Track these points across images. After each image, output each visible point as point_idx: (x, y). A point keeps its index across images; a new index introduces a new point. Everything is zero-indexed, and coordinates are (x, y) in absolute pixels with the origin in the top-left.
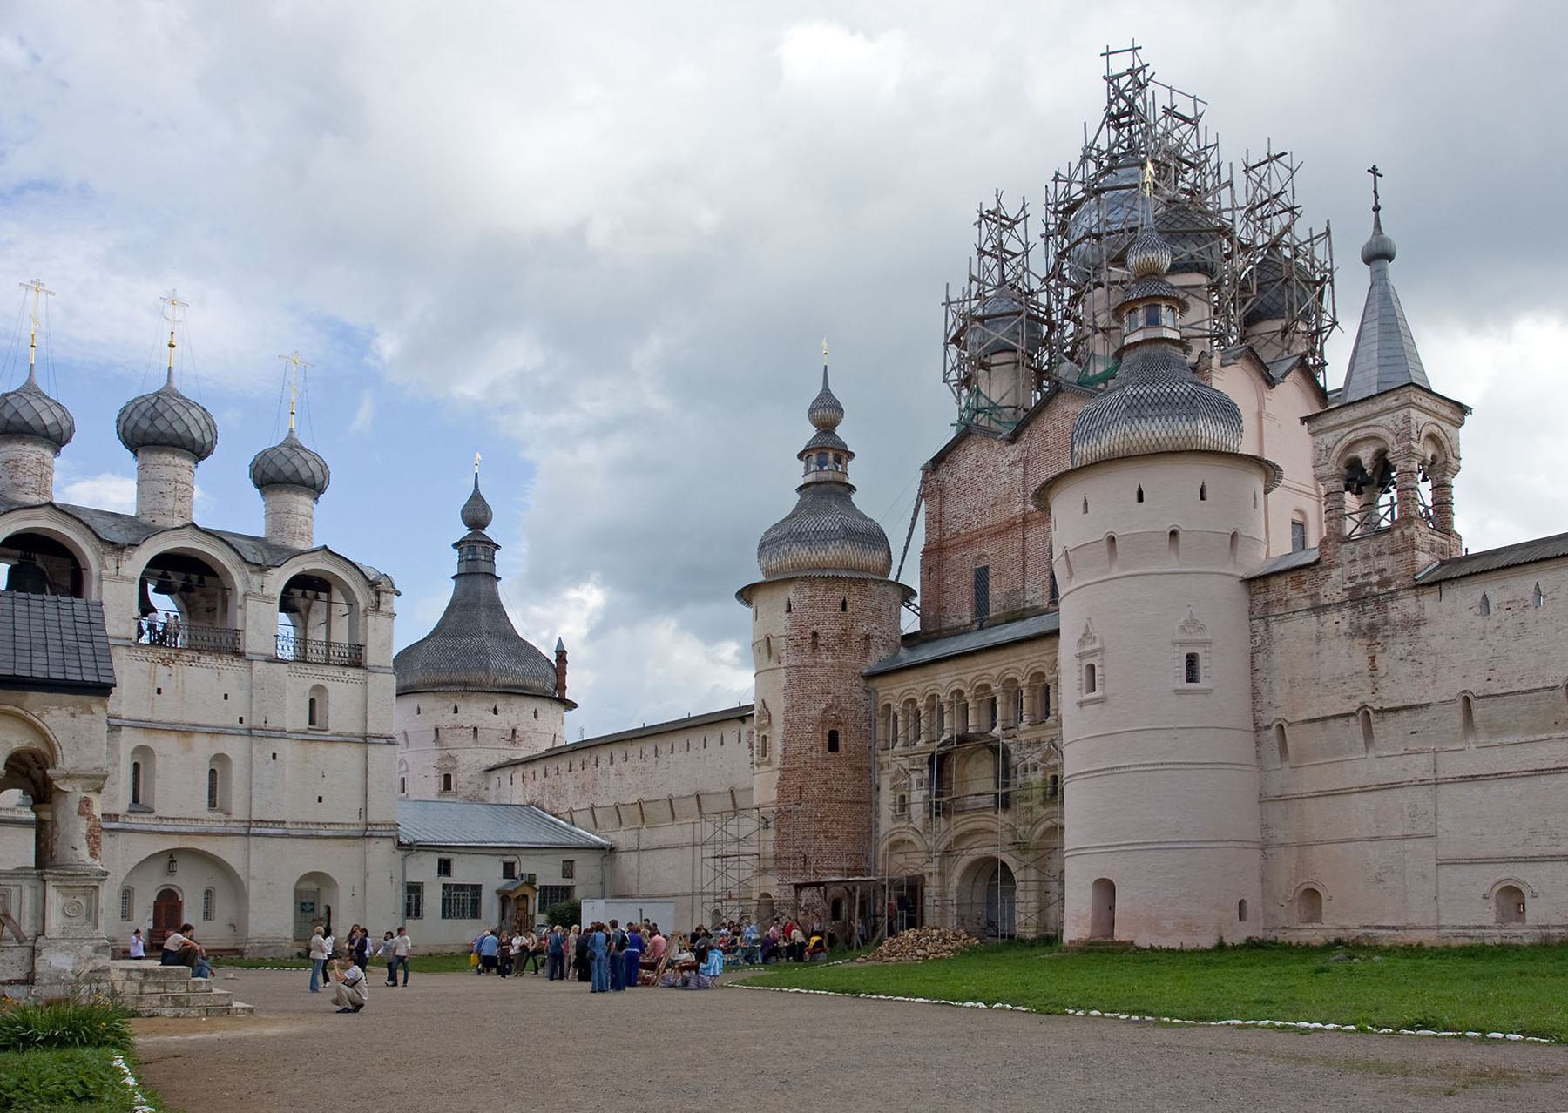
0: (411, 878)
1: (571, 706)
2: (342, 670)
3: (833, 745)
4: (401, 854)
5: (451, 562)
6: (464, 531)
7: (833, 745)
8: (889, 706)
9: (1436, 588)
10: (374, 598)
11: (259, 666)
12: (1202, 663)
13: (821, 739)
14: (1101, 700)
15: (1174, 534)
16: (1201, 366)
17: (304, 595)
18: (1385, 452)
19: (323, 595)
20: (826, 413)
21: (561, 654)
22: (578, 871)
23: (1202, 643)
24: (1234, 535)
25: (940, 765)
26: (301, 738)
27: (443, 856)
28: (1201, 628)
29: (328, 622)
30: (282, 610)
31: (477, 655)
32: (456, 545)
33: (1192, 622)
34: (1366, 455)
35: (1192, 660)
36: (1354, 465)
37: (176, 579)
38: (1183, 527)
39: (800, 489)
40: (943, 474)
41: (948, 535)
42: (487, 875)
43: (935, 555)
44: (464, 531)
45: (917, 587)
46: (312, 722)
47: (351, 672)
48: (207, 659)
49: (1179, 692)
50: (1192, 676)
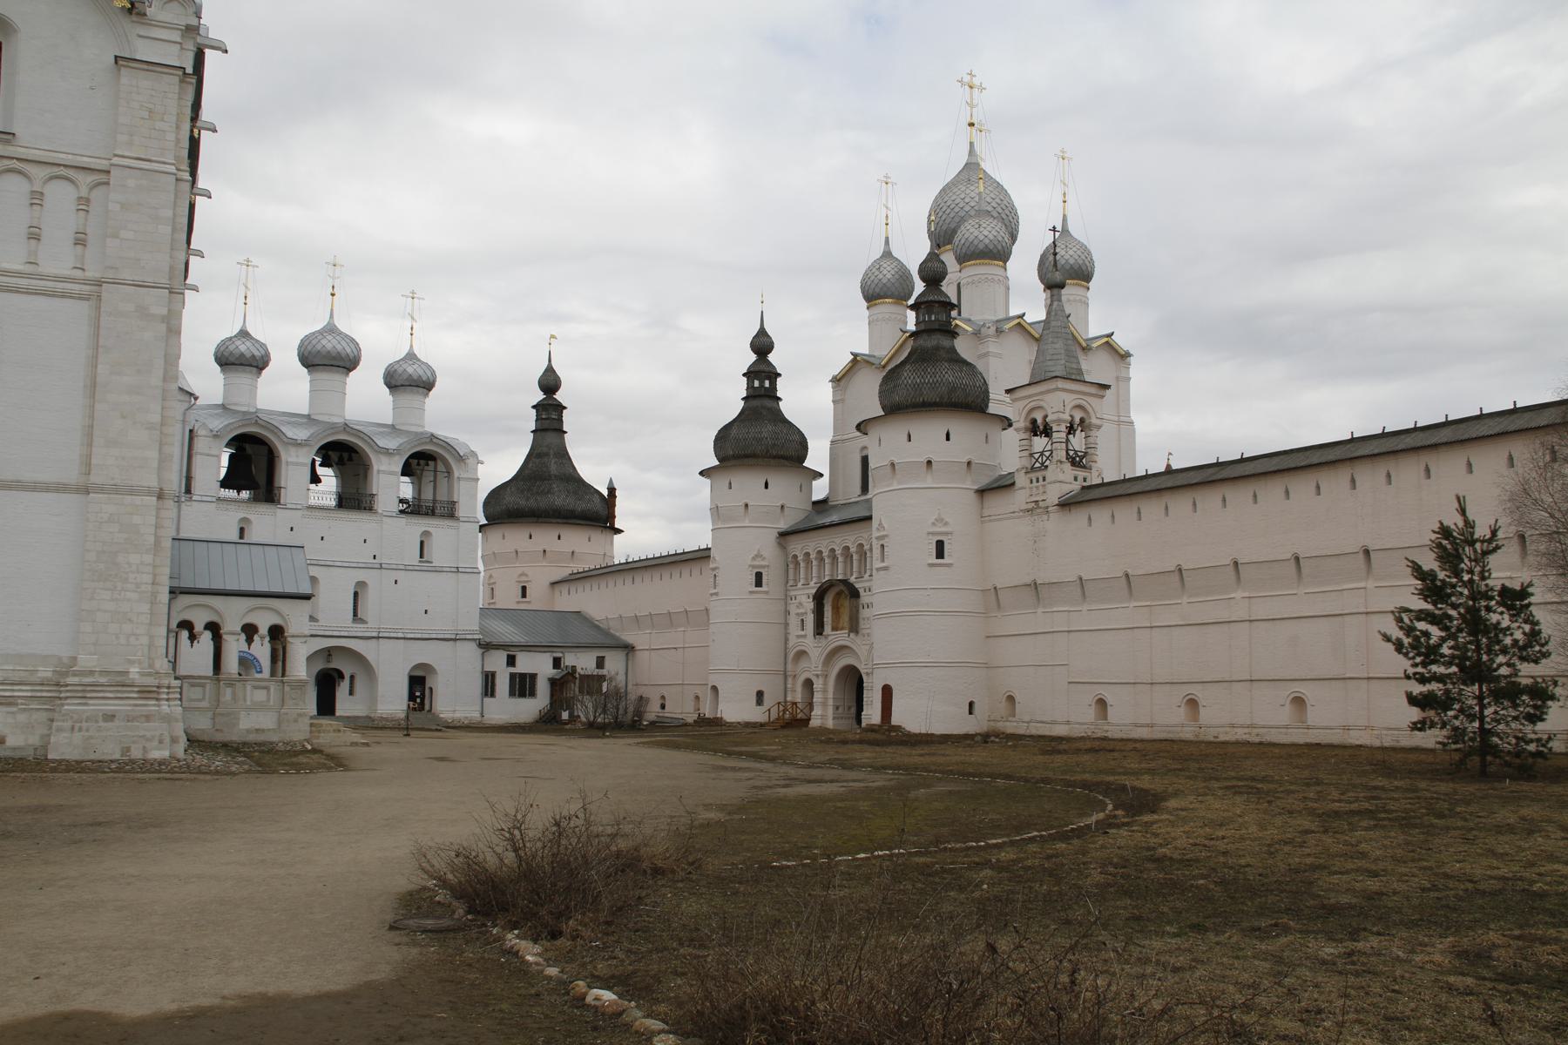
0: (488, 668)
1: (619, 531)
3: (759, 583)
6: (540, 396)
7: (759, 583)
12: (946, 547)
14: (886, 568)
15: (929, 462)
20: (762, 345)
21: (612, 490)
22: (608, 663)
23: (947, 534)
25: (819, 598)
28: (946, 524)
29: (435, 481)
30: (403, 474)
31: (550, 495)
33: (940, 520)
34: (1039, 417)
35: (940, 546)
36: (1034, 421)
37: (334, 456)
38: (934, 458)
42: (540, 666)
44: (540, 396)
45: (824, 469)
50: (940, 554)
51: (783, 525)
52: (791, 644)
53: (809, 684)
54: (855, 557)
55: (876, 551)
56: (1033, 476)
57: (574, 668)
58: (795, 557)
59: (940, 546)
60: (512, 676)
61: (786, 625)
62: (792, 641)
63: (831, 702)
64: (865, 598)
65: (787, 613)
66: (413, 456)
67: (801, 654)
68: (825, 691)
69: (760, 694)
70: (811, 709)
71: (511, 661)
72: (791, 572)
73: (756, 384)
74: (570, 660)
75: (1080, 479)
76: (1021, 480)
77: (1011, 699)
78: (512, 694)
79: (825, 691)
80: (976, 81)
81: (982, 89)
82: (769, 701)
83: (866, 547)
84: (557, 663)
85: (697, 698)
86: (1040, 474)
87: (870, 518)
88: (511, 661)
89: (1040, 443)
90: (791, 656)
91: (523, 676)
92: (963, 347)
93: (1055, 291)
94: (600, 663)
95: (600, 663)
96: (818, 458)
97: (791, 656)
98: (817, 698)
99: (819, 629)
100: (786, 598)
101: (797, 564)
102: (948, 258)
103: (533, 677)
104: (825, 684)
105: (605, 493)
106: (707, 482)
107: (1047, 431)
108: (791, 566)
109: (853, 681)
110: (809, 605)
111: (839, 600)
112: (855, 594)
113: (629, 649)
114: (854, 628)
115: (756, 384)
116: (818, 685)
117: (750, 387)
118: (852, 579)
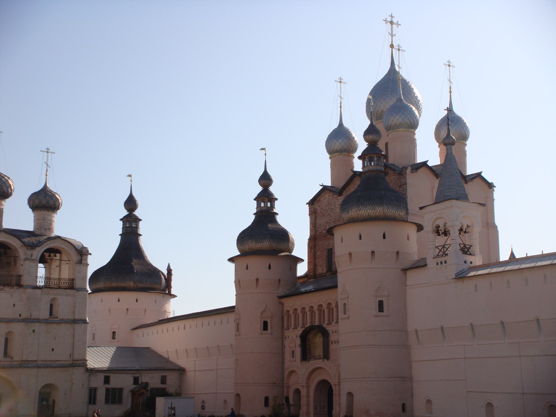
1: (174, 296)
2: (65, 290)
4: (87, 374)
5: (119, 228)
6: (125, 213)
8: (288, 311)
9: (461, 280)
10: (80, 258)
11: (30, 291)
12: (385, 304)
13: (260, 326)
16: (403, 173)
17: (50, 256)
18: (446, 223)
19: (58, 255)
21: (169, 271)
24: (398, 253)
25: (304, 337)
26: (46, 322)
27: (106, 374)
29: (60, 266)
32: (121, 220)
34: (441, 223)
35: (381, 304)
36: (438, 227)
39: (255, 214)
40: (316, 206)
41: (318, 233)
43: (314, 242)
44: (125, 213)
46: (51, 314)
47: (68, 291)
48: (7, 289)
49: (376, 316)
51: (281, 292)
52: (286, 366)
53: (297, 391)
54: (326, 311)
55: (341, 307)
56: (439, 260)
57: (147, 384)
58: (288, 311)
59: (381, 304)
60: (107, 390)
61: (283, 354)
62: (287, 363)
63: (312, 403)
64: (332, 338)
65: (283, 347)
66: (46, 251)
67: (292, 372)
68: (308, 396)
69: (267, 399)
70: (300, 409)
71: (107, 380)
72: (285, 321)
73: (262, 205)
74: (145, 378)
75: (468, 262)
76: (431, 262)
77: (429, 401)
78: (107, 401)
79: (308, 396)
80: (395, 20)
81: (398, 24)
82: (271, 403)
83: (333, 305)
84: (136, 380)
85: (225, 401)
86: (443, 259)
87: (336, 287)
88: (107, 380)
89: (441, 240)
90: (286, 374)
91: (114, 389)
92: (391, 179)
93: (449, 147)
94: (163, 380)
95: (163, 380)
96: (301, 249)
97: (286, 374)
98: (304, 401)
99: (306, 356)
100: (283, 338)
101: (289, 316)
102: (380, 126)
103: (121, 390)
104: (308, 392)
105: (165, 273)
106: (232, 266)
107: (446, 233)
108: (286, 317)
109: (326, 390)
110: (298, 342)
111: (315, 339)
112: (325, 334)
113: (181, 371)
114: (326, 355)
115: (262, 205)
116: (304, 392)
117: (258, 206)
118: (324, 326)
